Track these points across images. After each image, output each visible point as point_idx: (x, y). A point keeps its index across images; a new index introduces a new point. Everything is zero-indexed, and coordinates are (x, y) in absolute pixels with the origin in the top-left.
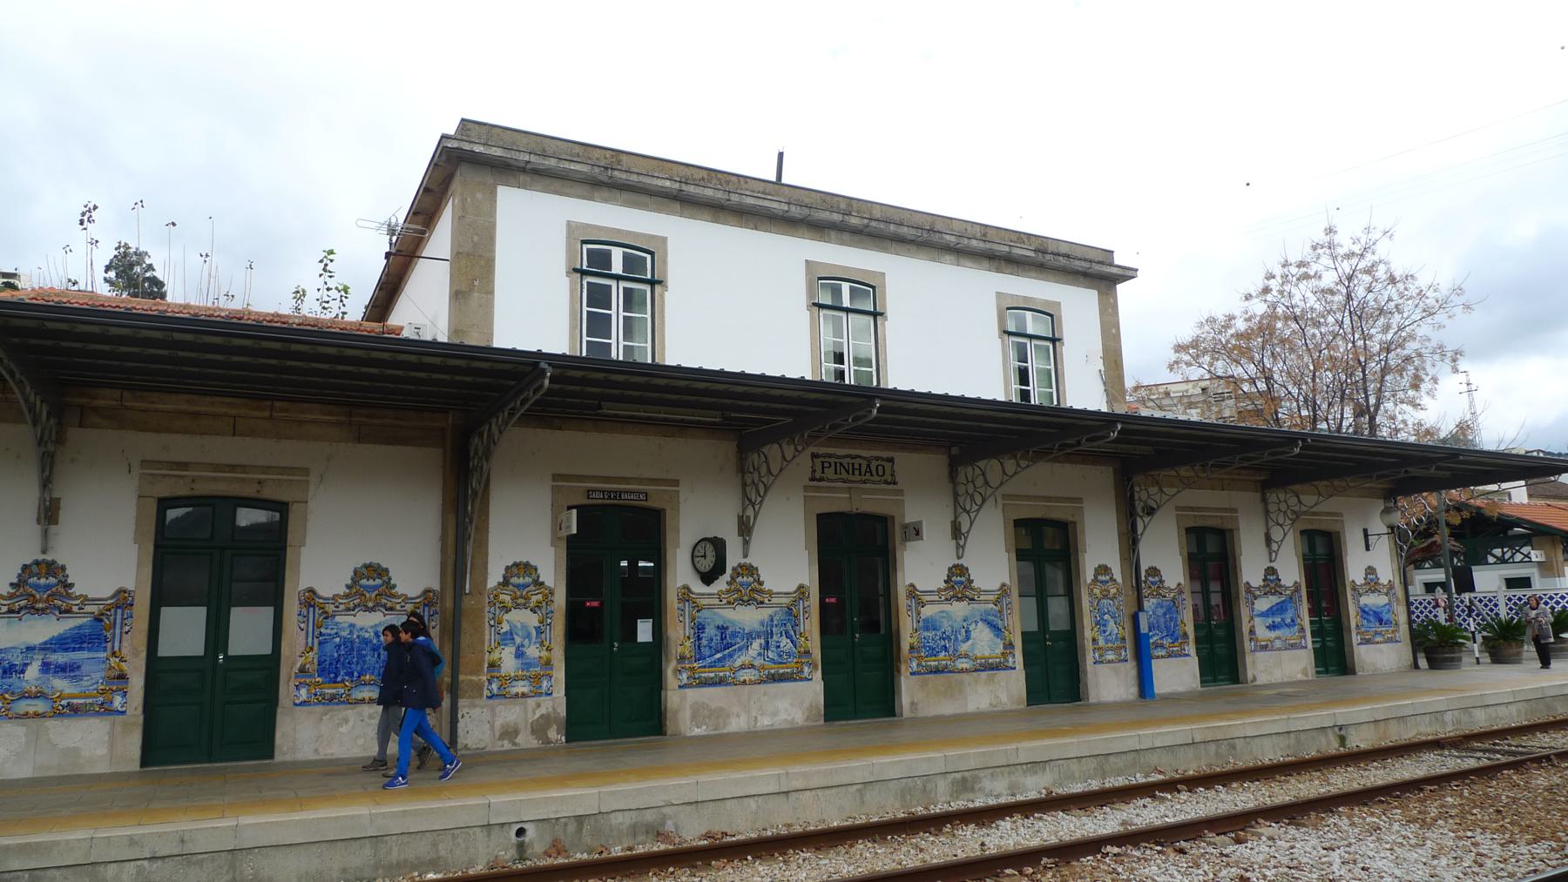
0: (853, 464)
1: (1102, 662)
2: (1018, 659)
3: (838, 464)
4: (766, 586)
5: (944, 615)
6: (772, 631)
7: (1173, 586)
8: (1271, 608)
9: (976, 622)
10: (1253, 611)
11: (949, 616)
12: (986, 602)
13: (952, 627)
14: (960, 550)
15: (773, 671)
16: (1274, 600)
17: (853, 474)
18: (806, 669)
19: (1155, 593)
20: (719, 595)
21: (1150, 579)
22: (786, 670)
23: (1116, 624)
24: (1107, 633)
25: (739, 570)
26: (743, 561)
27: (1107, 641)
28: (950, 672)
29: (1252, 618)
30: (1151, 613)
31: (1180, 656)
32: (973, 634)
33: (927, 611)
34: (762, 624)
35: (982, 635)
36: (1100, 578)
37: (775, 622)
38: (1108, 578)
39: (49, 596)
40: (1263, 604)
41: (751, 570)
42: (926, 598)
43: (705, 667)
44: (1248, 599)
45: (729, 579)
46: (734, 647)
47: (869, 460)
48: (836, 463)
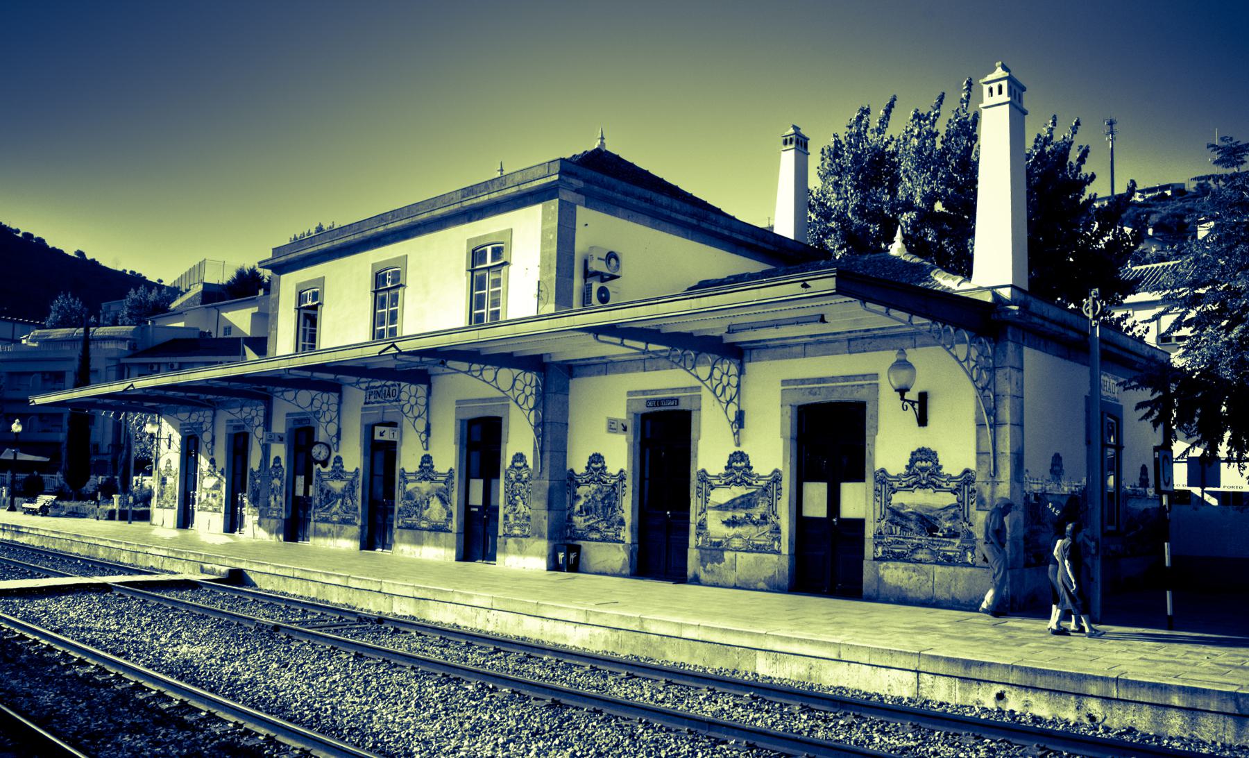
2: (454, 525)
4: (345, 469)
7: (615, 472)
8: (733, 500)
9: (433, 496)
10: (707, 502)
12: (440, 481)
14: (426, 444)
16: (739, 491)
19: (596, 479)
21: (593, 465)
23: (524, 503)
27: (516, 518)
28: (417, 529)
29: (704, 510)
30: (590, 497)
32: (431, 505)
33: (410, 487)
35: (436, 505)
38: (522, 464)
39: (928, 475)
40: (722, 496)
44: (702, 489)
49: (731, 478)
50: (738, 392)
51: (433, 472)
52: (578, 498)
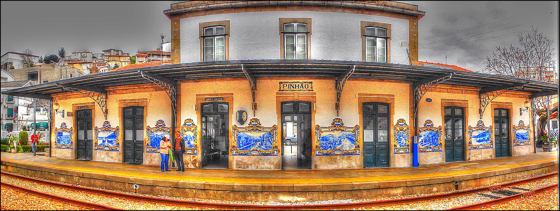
0: (296, 85)
1: (398, 153)
3: (290, 85)
4: (262, 125)
5: (331, 136)
6: (264, 140)
10: (471, 136)
11: (332, 136)
13: (334, 140)
15: (264, 152)
16: (481, 132)
17: (296, 88)
18: (276, 152)
19: (429, 129)
20: (246, 128)
21: (427, 124)
22: (269, 152)
23: (405, 140)
24: (401, 143)
25: (253, 120)
26: (254, 118)
28: (332, 155)
30: (426, 136)
31: (438, 151)
32: (342, 143)
33: (324, 134)
34: (260, 137)
36: (400, 123)
37: (265, 137)
40: (475, 133)
41: (256, 120)
42: (323, 130)
43: (241, 150)
45: (249, 123)
46: (250, 144)
47: (302, 83)
48: (289, 85)
49: (478, 128)
50: (106, 103)
51: (344, 127)
52: (421, 136)
